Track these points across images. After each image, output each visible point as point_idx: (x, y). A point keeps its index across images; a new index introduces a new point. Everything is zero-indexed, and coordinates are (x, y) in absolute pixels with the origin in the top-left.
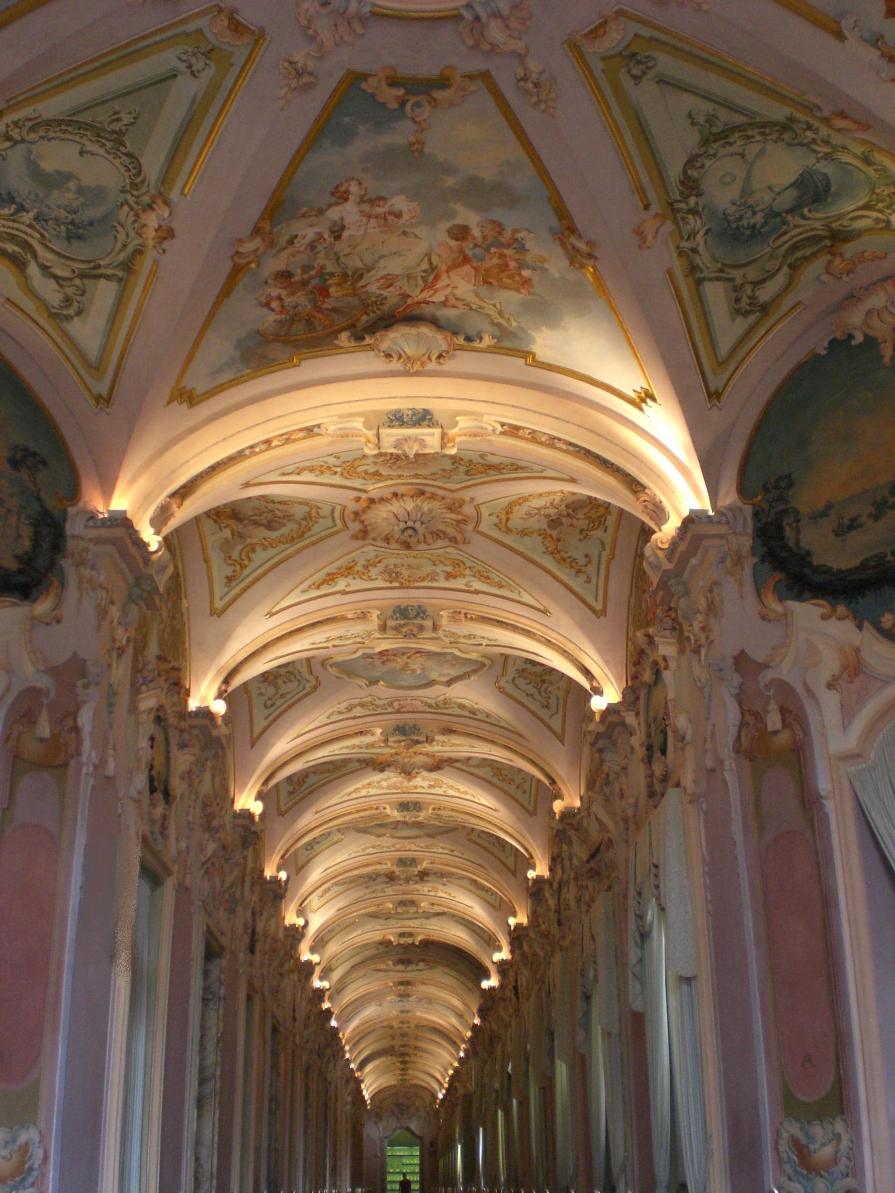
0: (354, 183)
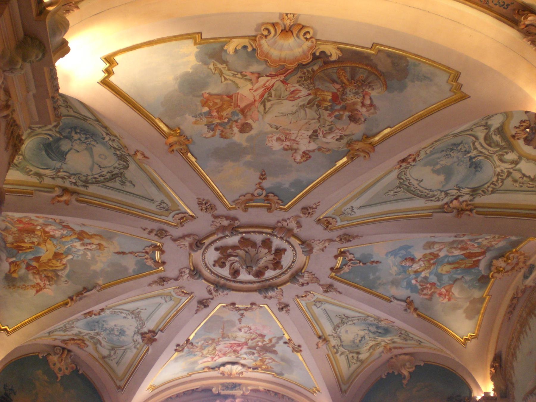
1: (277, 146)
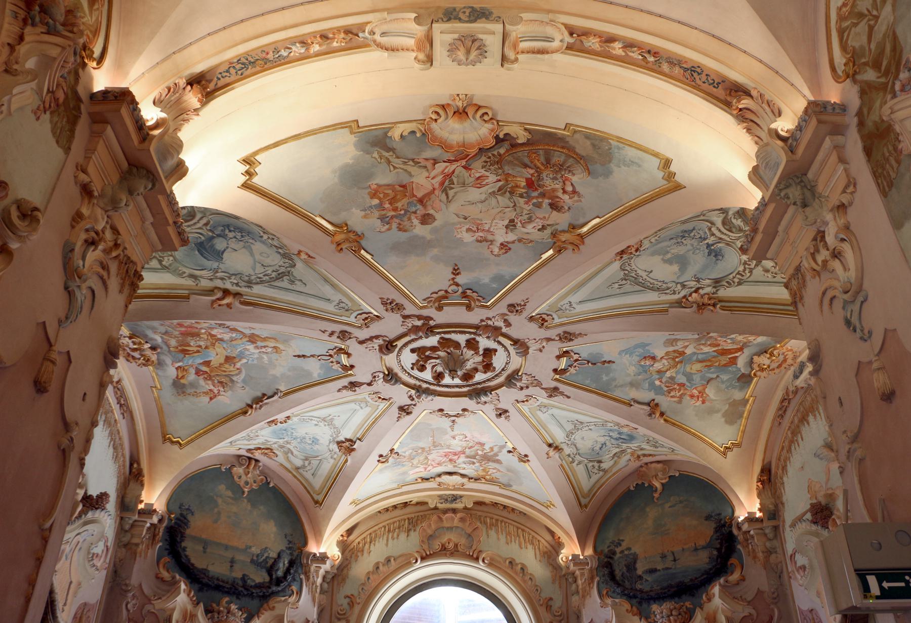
1: (468, 238)
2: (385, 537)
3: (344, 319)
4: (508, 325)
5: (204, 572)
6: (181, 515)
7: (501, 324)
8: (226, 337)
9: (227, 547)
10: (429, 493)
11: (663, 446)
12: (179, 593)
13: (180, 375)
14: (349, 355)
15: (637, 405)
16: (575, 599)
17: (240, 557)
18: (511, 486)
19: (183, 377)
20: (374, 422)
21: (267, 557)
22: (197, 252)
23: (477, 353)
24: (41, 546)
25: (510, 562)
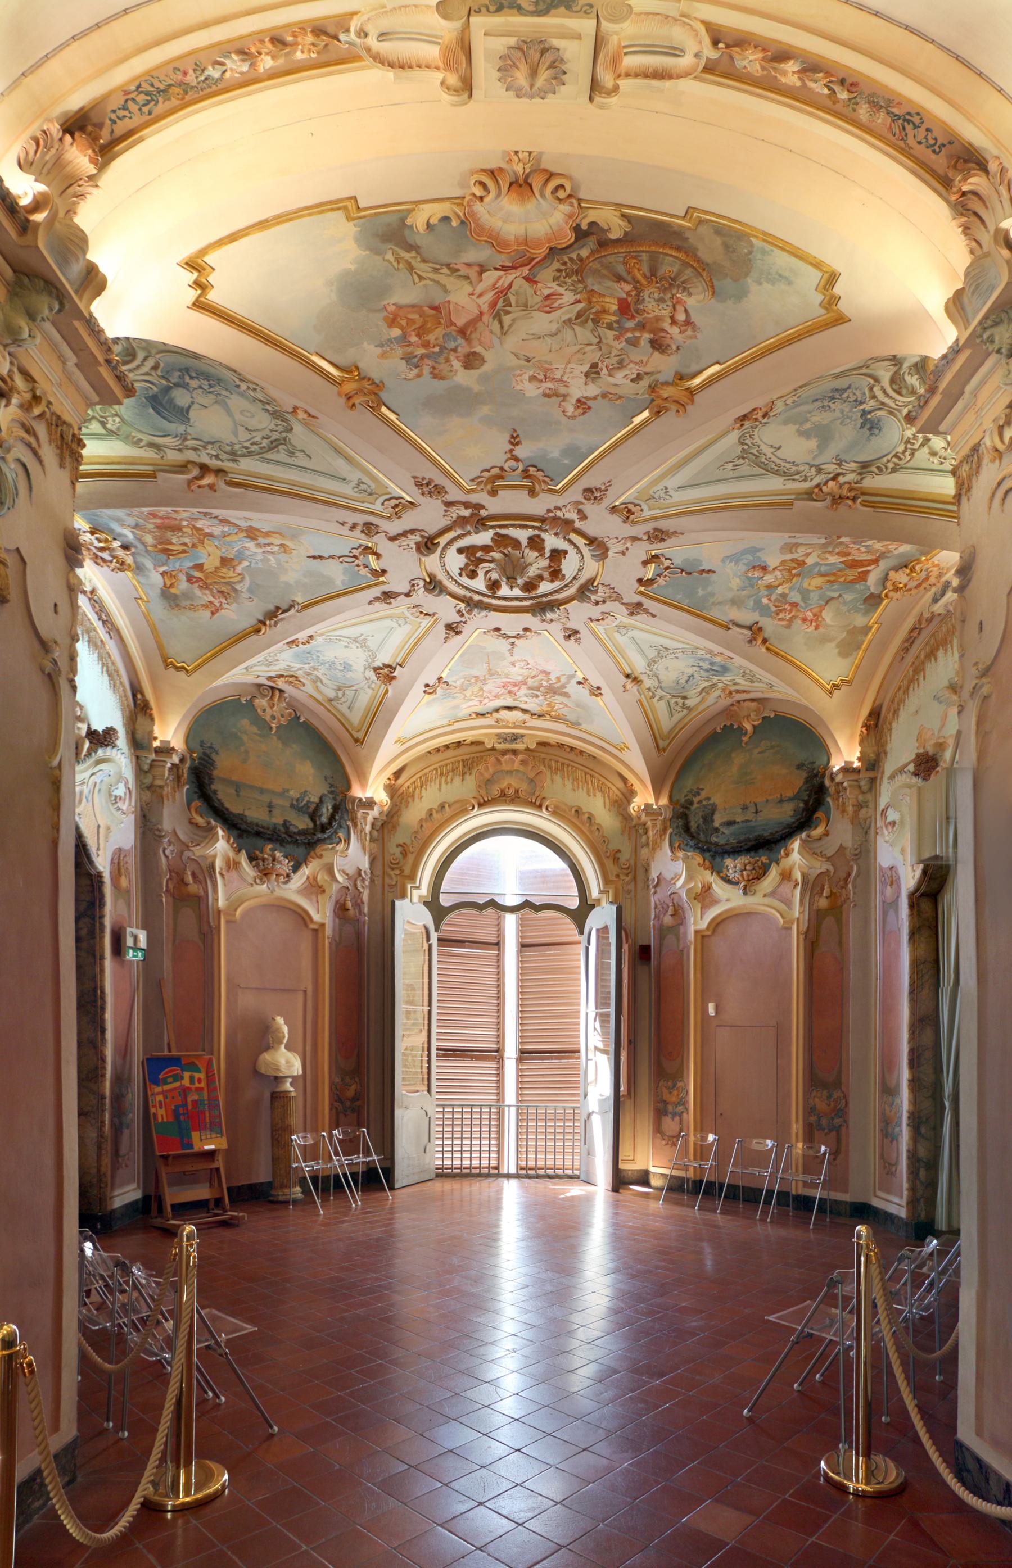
0: (569, 414)
1: (532, 390)
2: (438, 781)
3: (367, 506)
4: (583, 517)
5: (242, 817)
6: (204, 754)
7: (572, 515)
8: (217, 531)
9: (262, 791)
10: (484, 731)
11: (760, 681)
12: (218, 840)
13: (168, 583)
14: (378, 556)
15: (735, 629)
16: (644, 852)
17: (278, 801)
18: (579, 724)
19: (172, 585)
20: (416, 644)
21: (308, 802)
22: (151, 410)
23: (542, 555)
24: (54, 787)
25: (577, 811)
